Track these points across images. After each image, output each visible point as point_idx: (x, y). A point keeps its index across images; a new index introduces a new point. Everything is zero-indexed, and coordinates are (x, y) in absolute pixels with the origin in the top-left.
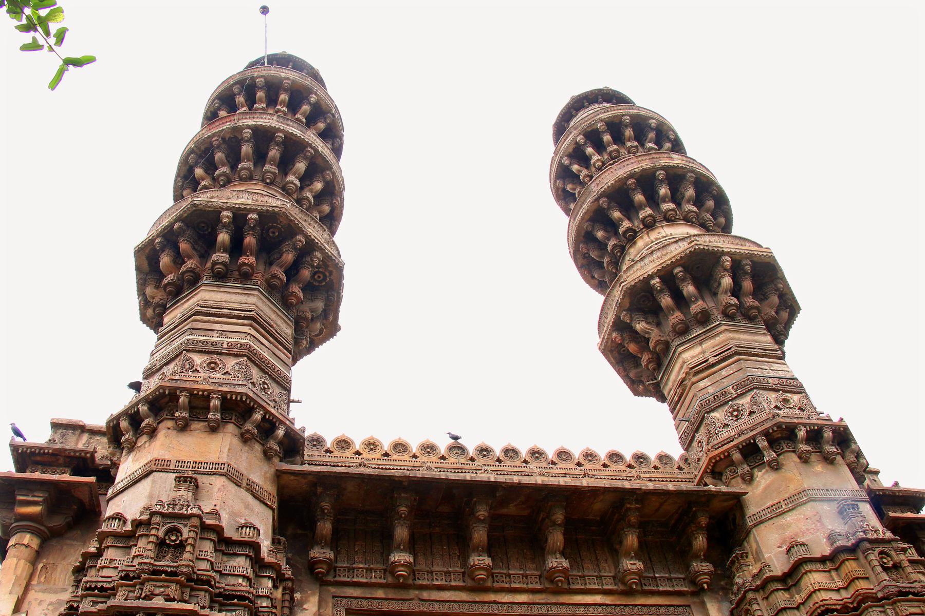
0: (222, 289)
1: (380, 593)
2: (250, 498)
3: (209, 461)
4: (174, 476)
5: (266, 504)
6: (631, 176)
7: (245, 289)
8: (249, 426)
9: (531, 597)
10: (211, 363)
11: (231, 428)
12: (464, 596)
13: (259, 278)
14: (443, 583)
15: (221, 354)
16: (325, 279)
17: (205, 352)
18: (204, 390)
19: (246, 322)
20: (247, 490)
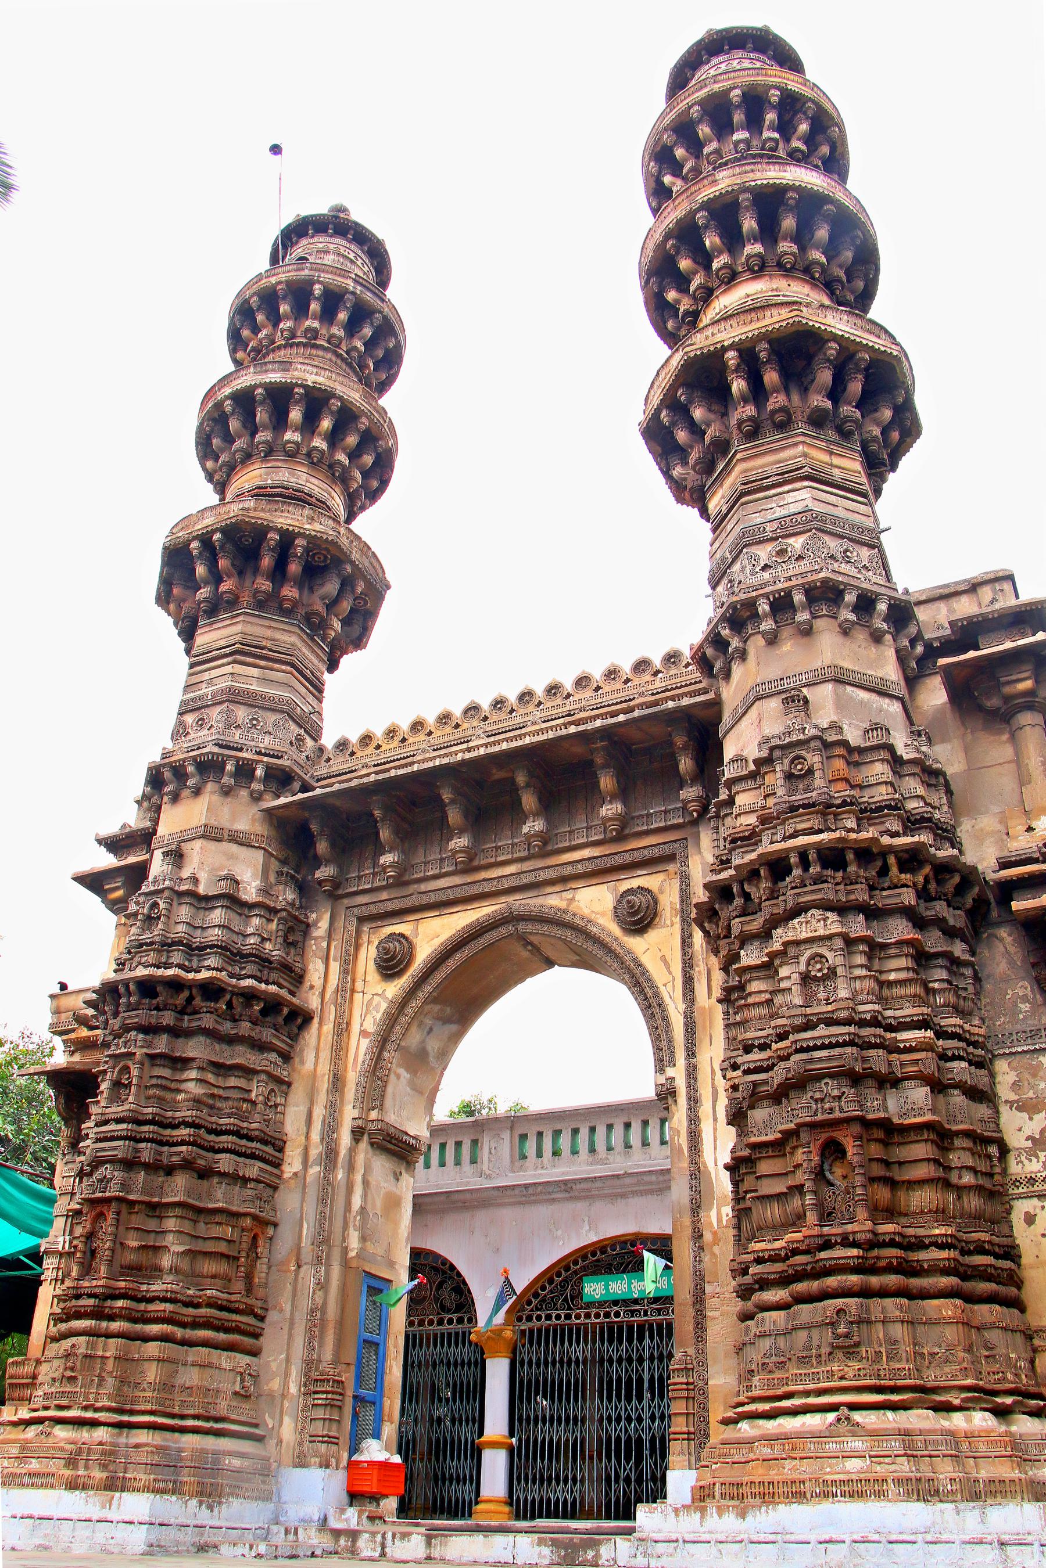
0: (215, 626)
1: (384, 895)
2: (234, 848)
3: (194, 826)
4: (161, 850)
5: (254, 847)
6: (668, 236)
7: (232, 617)
8: (225, 780)
9: (519, 866)
10: (200, 720)
11: (210, 786)
12: (457, 880)
13: (246, 598)
14: (437, 871)
15: (208, 706)
16: (326, 557)
17: (195, 710)
18: (179, 761)
19: (225, 661)
20: (230, 841)
